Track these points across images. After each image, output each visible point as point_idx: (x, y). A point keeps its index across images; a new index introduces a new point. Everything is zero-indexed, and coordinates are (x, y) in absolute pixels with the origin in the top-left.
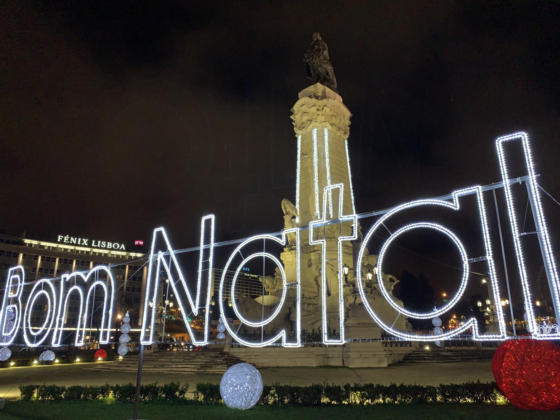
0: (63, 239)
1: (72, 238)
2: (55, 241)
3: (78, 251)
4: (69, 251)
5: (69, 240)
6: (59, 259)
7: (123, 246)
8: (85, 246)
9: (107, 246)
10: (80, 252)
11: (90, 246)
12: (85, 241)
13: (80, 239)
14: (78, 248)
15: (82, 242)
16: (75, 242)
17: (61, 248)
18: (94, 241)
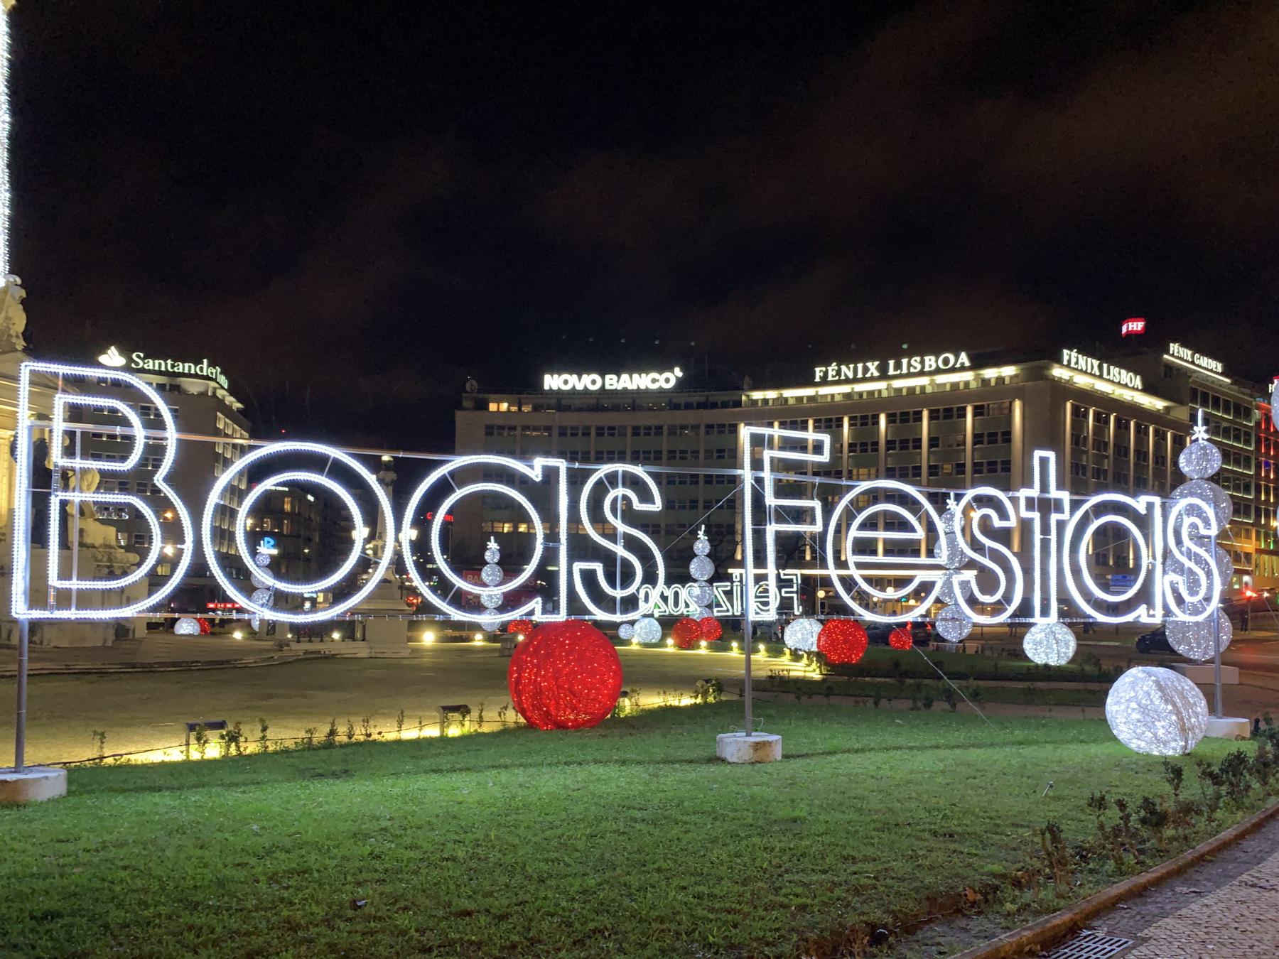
0: (826, 373)
1: (844, 368)
2: (810, 382)
3: (861, 394)
4: (838, 398)
5: (839, 373)
6: (815, 421)
7: (964, 358)
8: (872, 379)
9: (923, 367)
10: (865, 396)
11: (884, 375)
12: (873, 367)
13: (860, 366)
14: (859, 388)
15: (866, 370)
16: (851, 375)
17: (825, 396)
18: (891, 363)
